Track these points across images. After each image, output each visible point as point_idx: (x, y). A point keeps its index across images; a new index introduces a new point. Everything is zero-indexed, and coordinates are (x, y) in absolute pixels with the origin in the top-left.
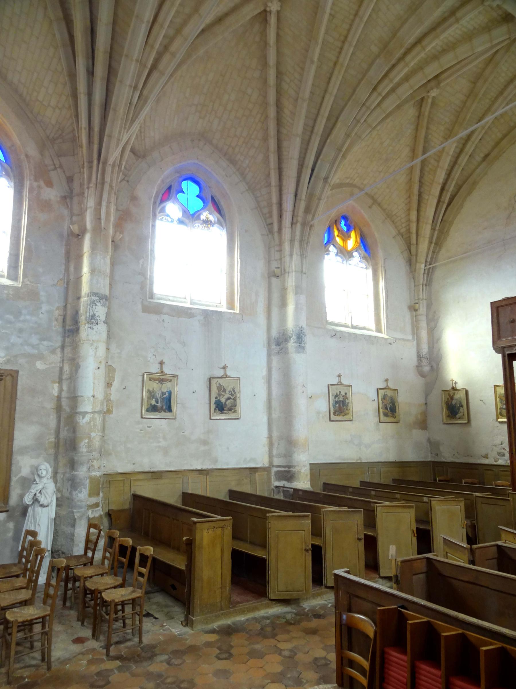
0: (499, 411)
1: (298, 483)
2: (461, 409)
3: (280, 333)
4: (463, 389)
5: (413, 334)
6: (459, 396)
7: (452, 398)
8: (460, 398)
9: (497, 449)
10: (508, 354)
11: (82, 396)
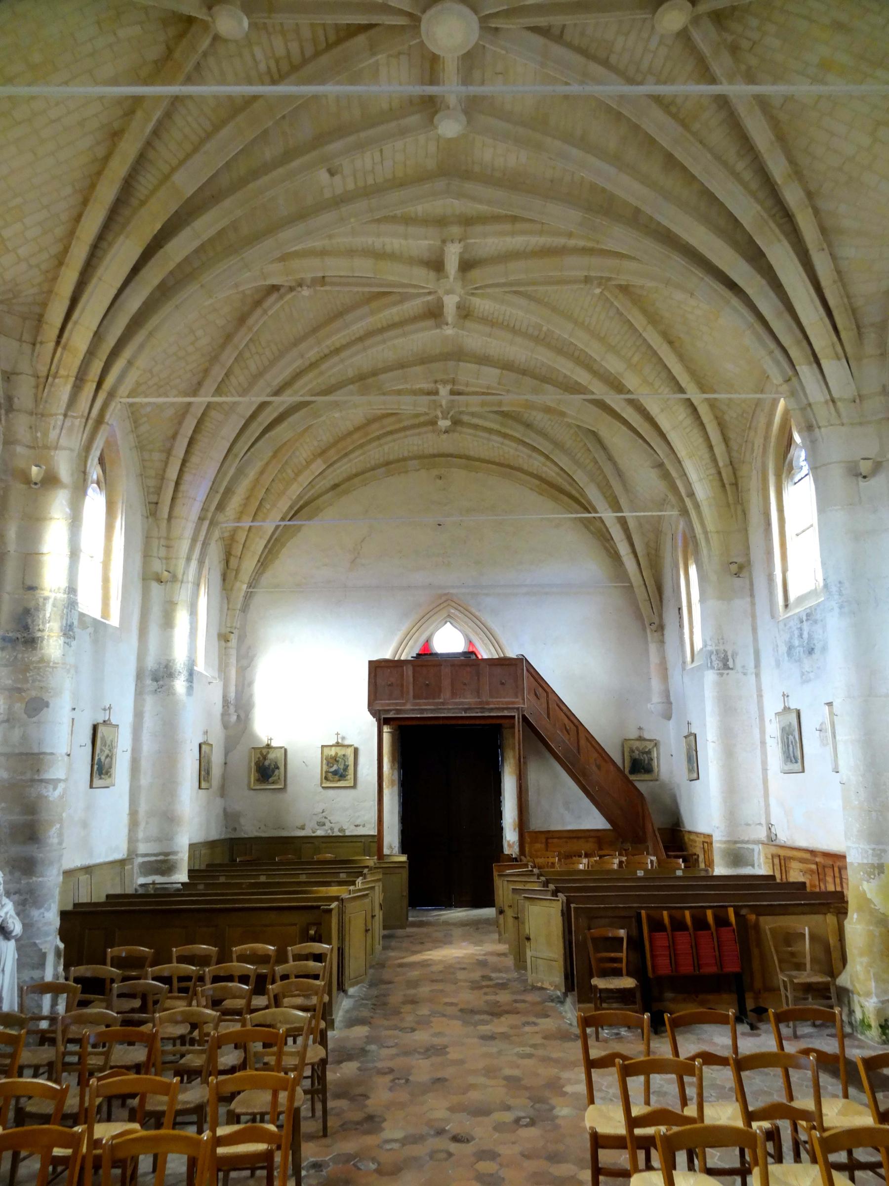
1: (180, 876)
2: (276, 772)
3: (159, 664)
4: (281, 748)
7: (265, 758)
10: (384, 718)
11: (52, 754)
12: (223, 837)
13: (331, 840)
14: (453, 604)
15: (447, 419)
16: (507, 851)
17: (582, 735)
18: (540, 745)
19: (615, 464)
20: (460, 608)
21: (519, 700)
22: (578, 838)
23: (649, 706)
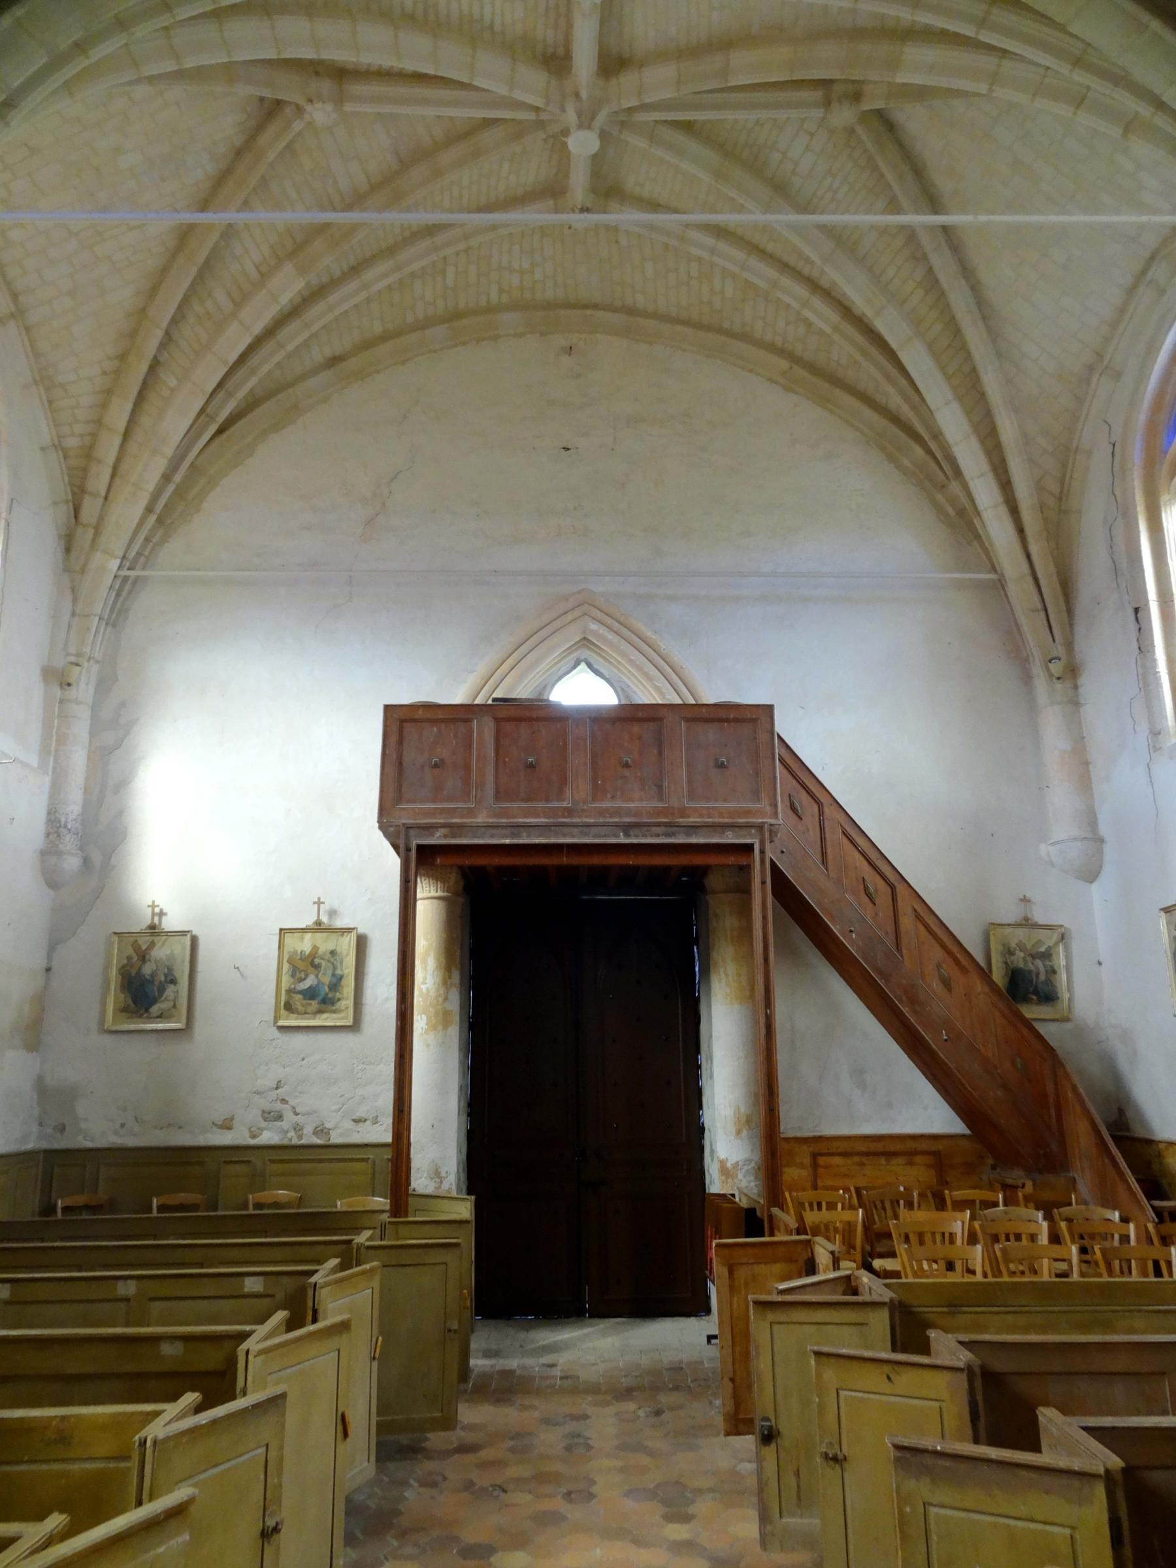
0: (283, 999)
2: (170, 990)
4: (183, 933)
5: (44, 751)
6: (168, 952)
7: (143, 957)
8: (171, 957)
9: (264, 1103)
10: (420, 848)
12: (30, 1146)
13: (294, 1155)
14: (599, 615)
15: (589, 128)
16: (715, 1184)
17: (905, 906)
18: (799, 936)
19: (975, 288)
20: (609, 621)
21: (764, 805)
22: (889, 1155)
23: (1043, 847)
